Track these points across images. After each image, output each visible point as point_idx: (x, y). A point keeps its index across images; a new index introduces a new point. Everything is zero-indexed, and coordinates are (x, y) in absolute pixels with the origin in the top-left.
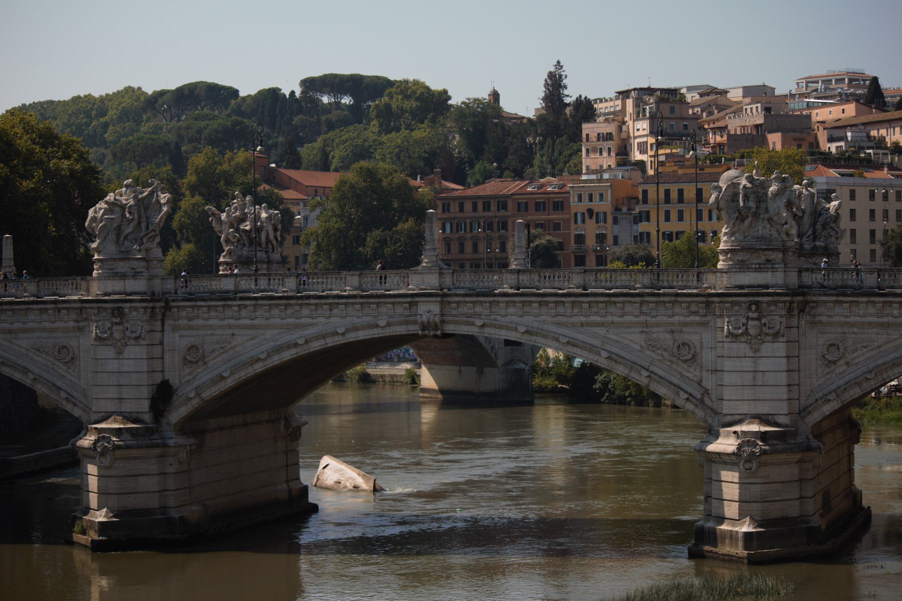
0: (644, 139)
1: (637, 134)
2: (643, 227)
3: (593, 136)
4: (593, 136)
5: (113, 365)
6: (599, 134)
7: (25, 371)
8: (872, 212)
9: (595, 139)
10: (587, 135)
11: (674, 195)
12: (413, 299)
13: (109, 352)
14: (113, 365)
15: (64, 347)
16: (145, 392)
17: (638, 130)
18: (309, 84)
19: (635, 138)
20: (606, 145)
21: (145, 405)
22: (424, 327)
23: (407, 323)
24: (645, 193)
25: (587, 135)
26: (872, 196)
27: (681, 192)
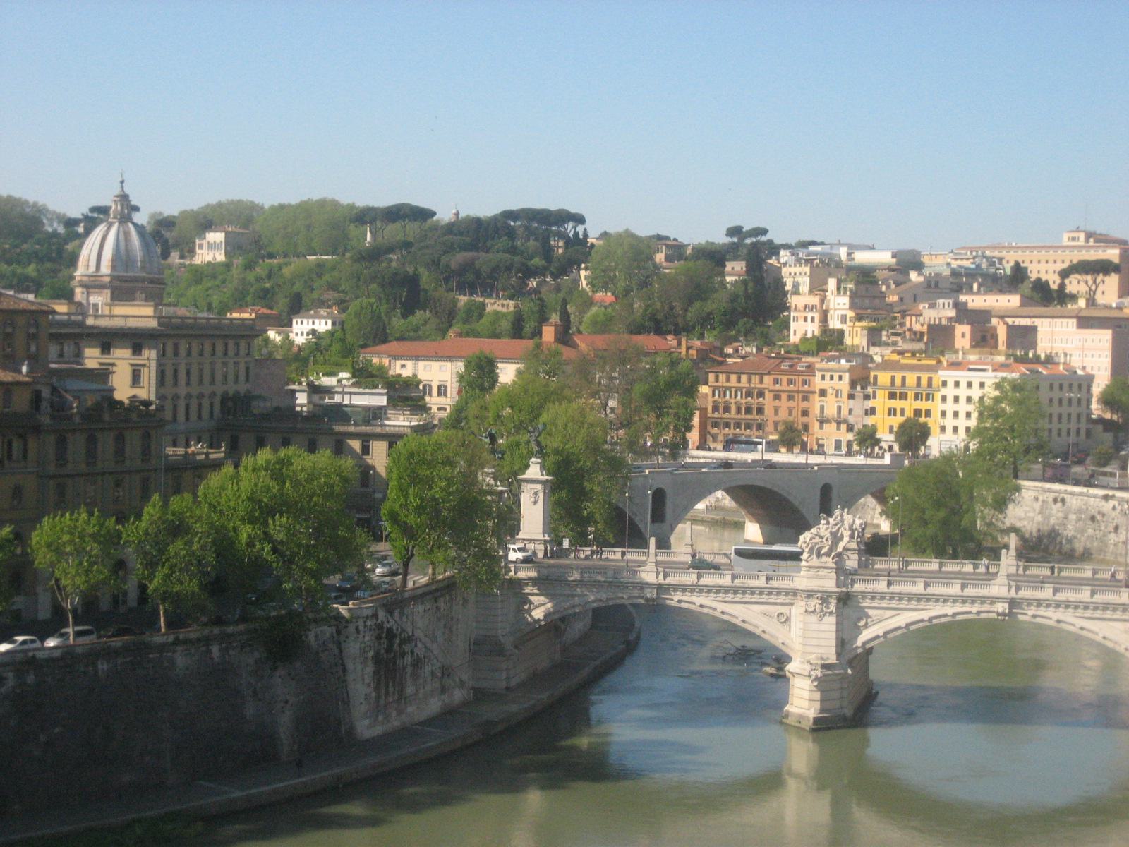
0: (844, 312)
1: (837, 307)
2: (870, 404)
3: (800, 306)
4: (800, 306)
5: (815, 627)
6: (806, 306)
7: (756, 626)
8: (1051, 400)
9: (802, 309)
10: (796, 306)
11: (898, 381)
12: (993, 600)
13: (814, 618)
14: (815, 627)
15: (781, 614)
16: (834, 643)
17: (839, 304)
18: (510, 215)
19: (835, 309)
20: (809, 315)
21: (834, 650)
22: (998, 614)
23: (988, 612)
24: (875, 377)
25: (796, 306)
26: (1051, 387)
27: (904, 379)
